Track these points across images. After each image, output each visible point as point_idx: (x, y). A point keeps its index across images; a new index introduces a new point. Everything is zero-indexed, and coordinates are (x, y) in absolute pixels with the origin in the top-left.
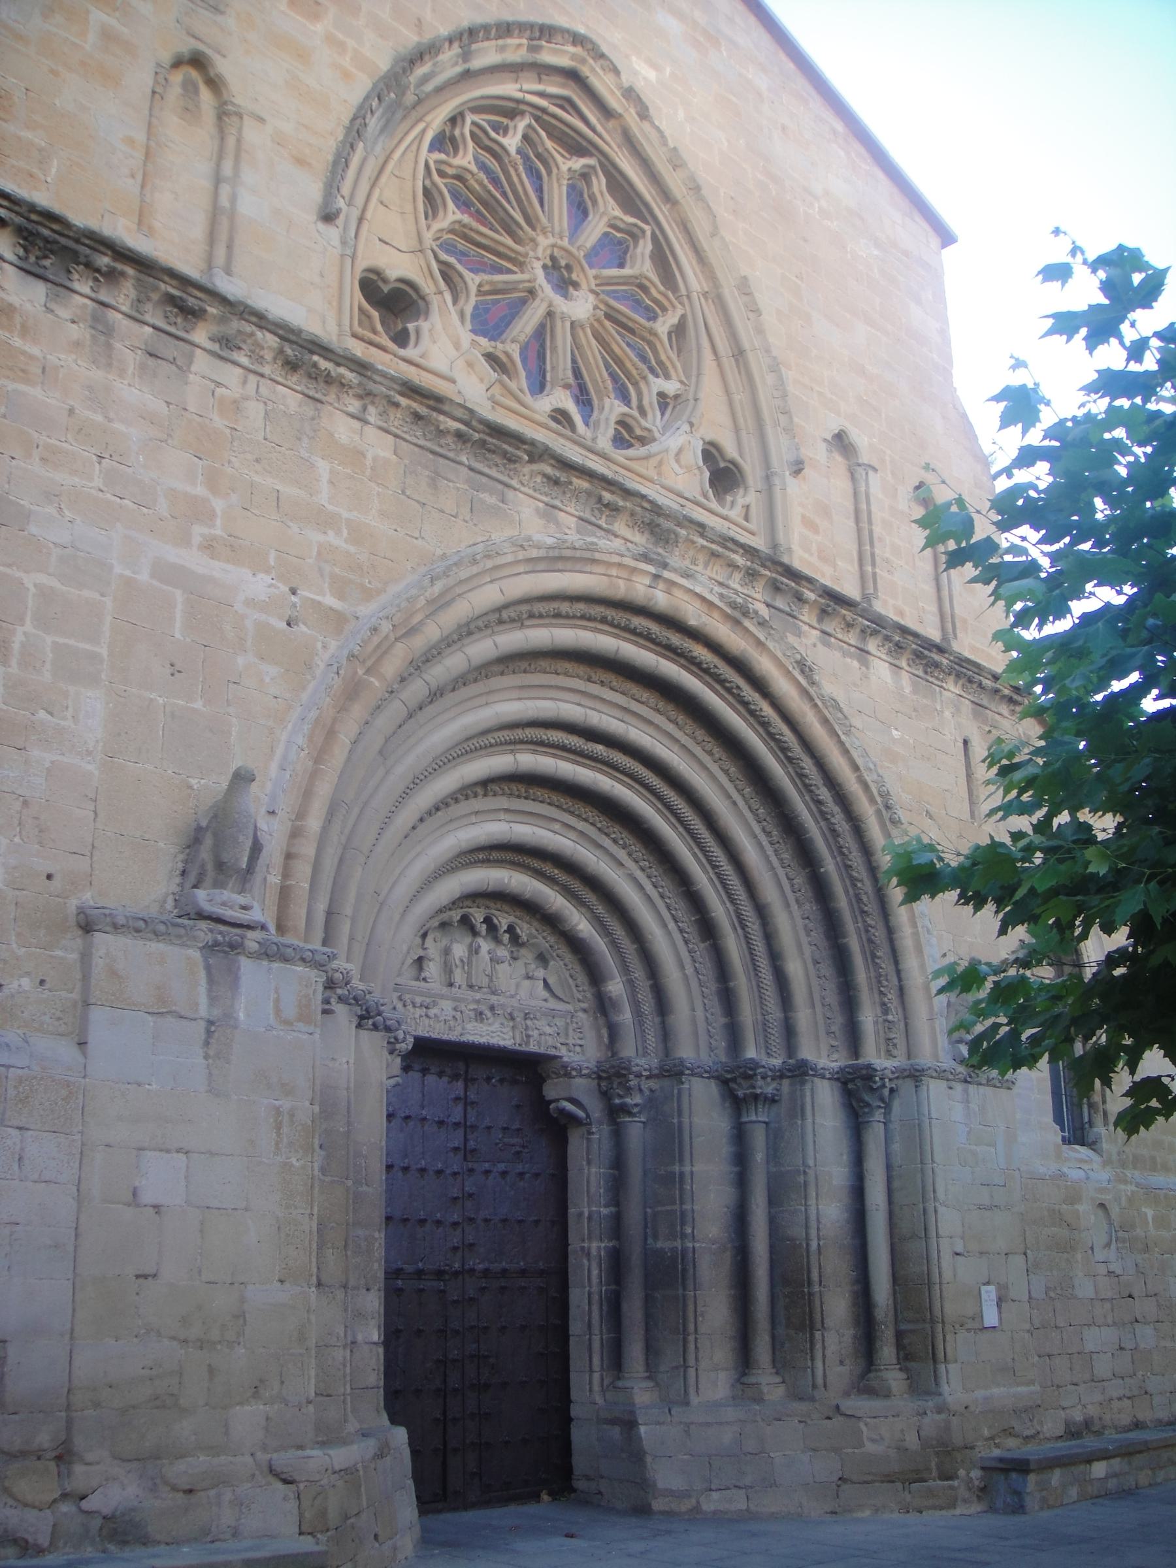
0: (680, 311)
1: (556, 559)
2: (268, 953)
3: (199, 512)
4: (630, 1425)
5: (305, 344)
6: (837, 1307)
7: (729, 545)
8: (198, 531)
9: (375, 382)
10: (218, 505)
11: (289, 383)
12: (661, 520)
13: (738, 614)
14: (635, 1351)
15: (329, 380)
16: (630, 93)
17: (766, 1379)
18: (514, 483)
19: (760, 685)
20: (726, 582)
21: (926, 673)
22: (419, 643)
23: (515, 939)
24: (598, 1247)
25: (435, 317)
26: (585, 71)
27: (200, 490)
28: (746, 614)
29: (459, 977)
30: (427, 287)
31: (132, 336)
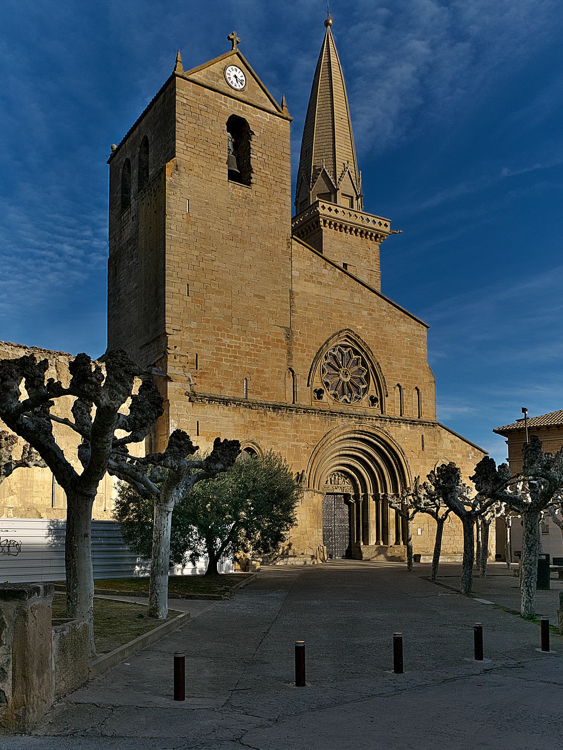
3: (296, 436)
10: (298, 435)
16: (356, 335)
23: (342, 476)
26: (348, 334)
29: (333, 483)
30: (323, 389)
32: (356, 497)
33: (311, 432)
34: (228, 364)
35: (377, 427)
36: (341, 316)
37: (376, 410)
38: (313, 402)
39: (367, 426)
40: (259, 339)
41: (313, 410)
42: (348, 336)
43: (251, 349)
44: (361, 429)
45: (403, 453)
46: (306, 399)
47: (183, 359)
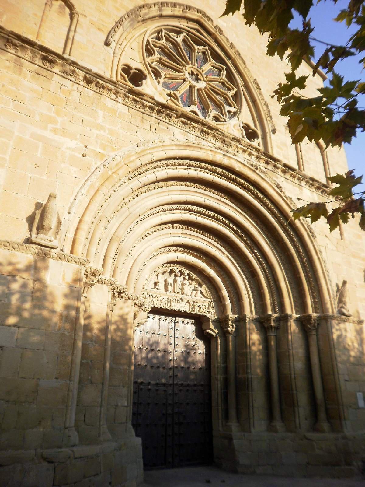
0: (235, 90)
4: (230, 439)
5: (94, 75)
6: (302, 398)
7: (250, 147)
8: (50, 126)
9: (120, 89)
10: (59, 119)
11: (89, 88)
12: (225, 138)
13: (254, 168)
14: (233, 412)
15: (103, 87)
16: (216, 27)
17: (278, 424)
18: (172, 123)
20: (250, 160)
21: (322, 194)
24: (220, 377)
27: (53, 114)
28: (256, 168)
32: (222, 323)
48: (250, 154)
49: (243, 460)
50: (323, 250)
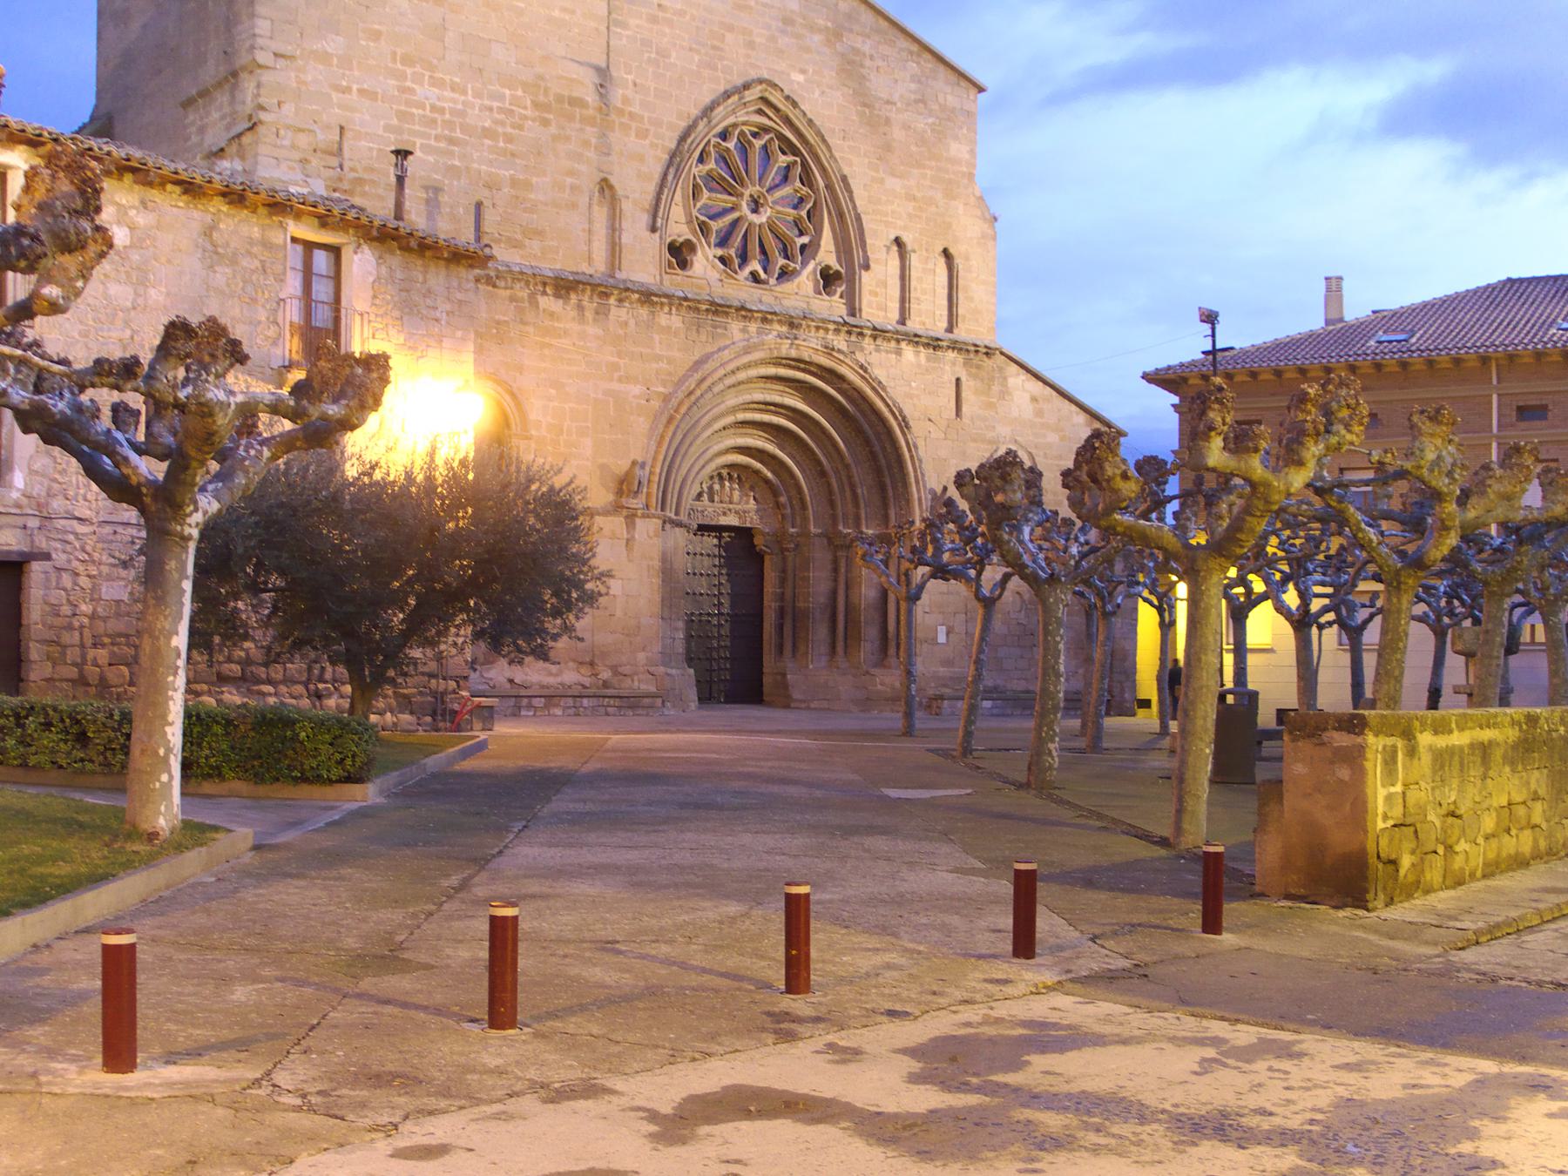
1: (747, 351)
2: (643, 516)
3: (615, 367)
4: (784, 675)
6: (871, 632)
8: (616, 375)
13: (829, 350)
16: (788, 98)
19: (842, 378)
22: (693, 398)
25: (699, 253)
26: (767, 95)
29: (716, 498)
31: (590, 305)
33: (658, 358)
34: (431, 159)
35: (839, 351)
36: (751, 45)
37: (834, 305)
38: (666, 277)
39: (810, 346)
40: (520, 93)
41: (666, 296)
42: (764, 100)
43: (496, 122)
44: (794, 353)
45: (905, 424)
46: (644, 264)
47: (303, 140)
48: (827, 330)
49: (796, 695)
50: (921, 443)
